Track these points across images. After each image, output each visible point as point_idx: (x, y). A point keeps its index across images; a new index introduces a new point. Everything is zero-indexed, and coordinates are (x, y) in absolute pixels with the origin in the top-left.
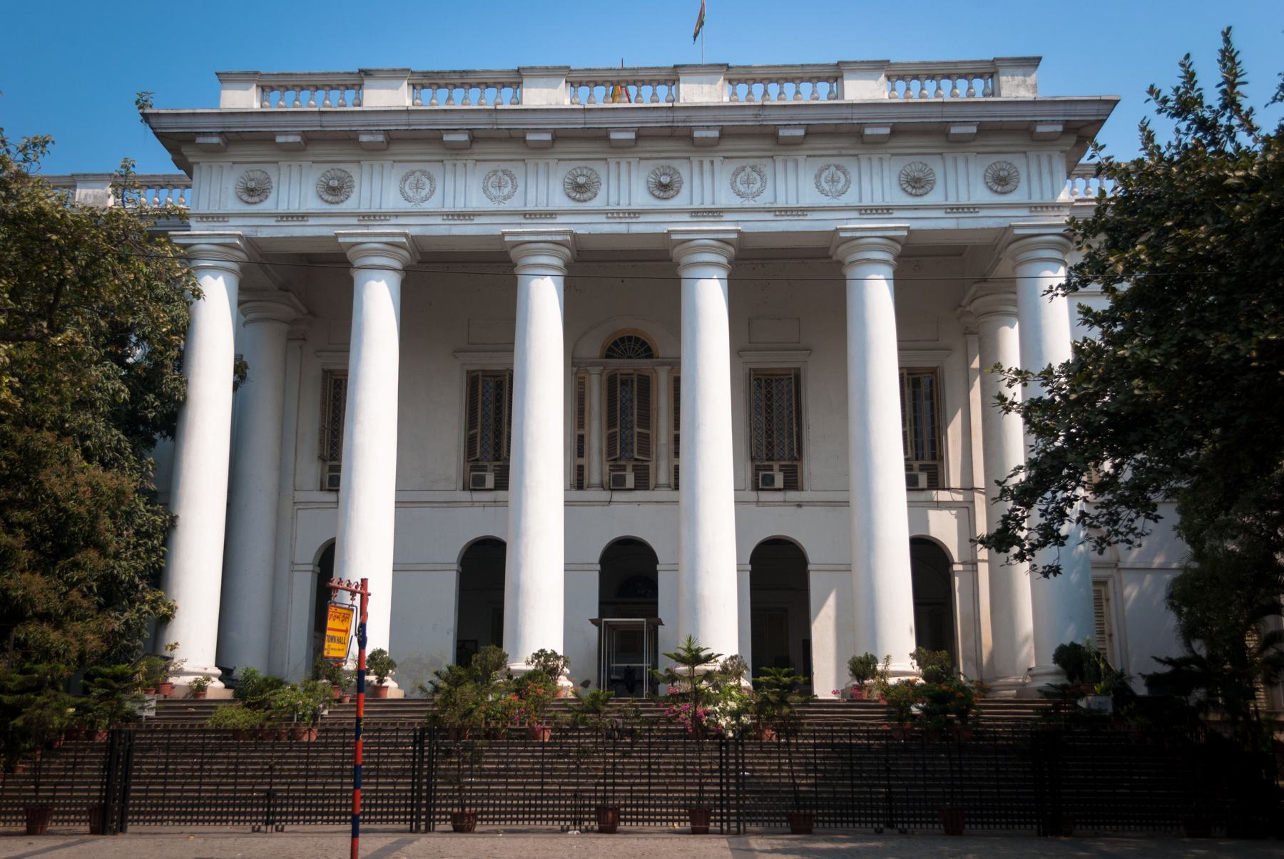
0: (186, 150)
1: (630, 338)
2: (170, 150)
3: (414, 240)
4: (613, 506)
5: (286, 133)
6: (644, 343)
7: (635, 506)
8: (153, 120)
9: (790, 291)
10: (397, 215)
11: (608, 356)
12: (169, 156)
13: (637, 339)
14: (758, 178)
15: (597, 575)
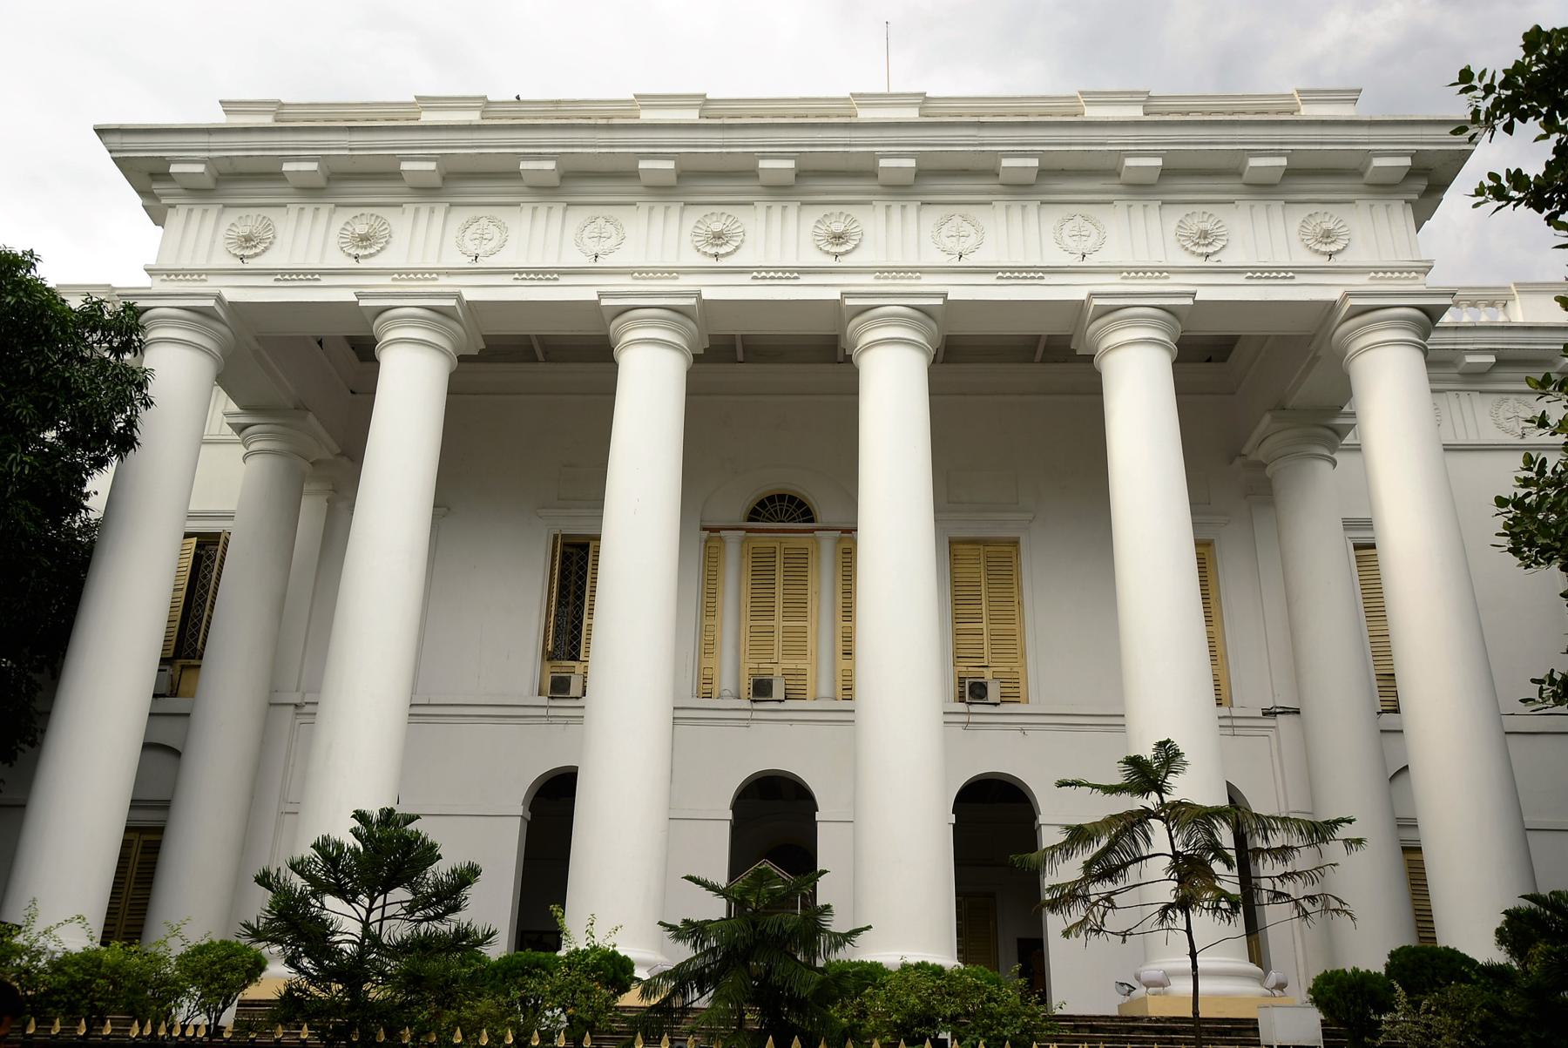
0: (157, 188)
1: (782, 497)
2: (141, 193)
3: (472, 306)
4: (754, 726)
5: (298, 159)
6: (801, 504)
7: (786, 726)
8: (115, 140)
9: (1016, 395)
10: (449, 272)
11: (750, 520)
12: (138, 201)
13: (792, 499)
14: (972, 230)
15: (727, 827)
